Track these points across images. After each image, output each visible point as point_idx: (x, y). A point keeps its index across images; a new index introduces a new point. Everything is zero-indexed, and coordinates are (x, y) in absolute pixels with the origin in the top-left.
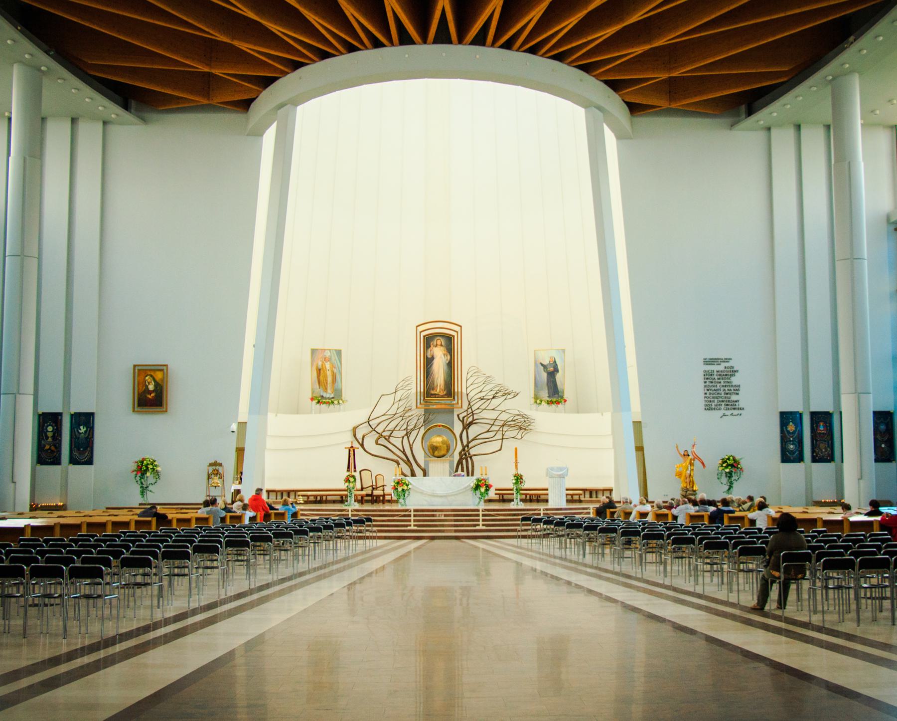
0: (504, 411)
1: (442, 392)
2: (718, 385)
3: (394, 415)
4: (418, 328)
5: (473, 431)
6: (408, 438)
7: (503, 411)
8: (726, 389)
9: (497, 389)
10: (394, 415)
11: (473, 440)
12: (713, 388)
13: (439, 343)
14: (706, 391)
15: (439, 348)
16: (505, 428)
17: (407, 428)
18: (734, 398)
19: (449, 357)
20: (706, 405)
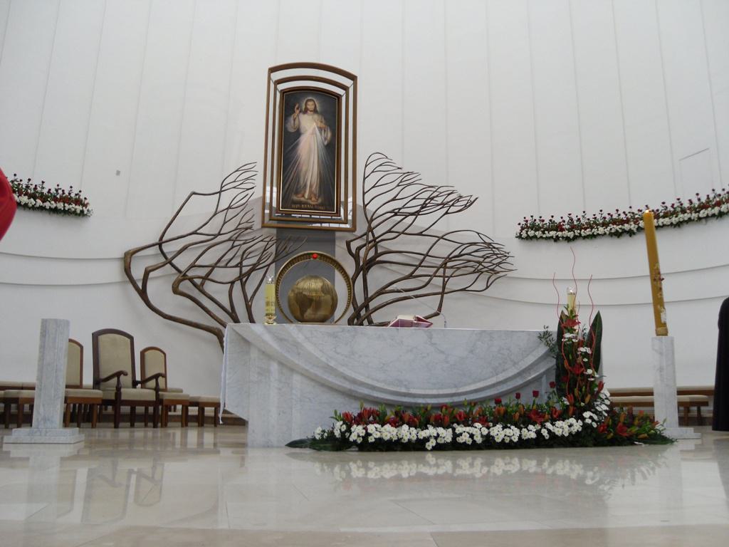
0: (442, 238)
1: (313, 199)
3: (216, 236)
4: (272, 74)
5: (377, 277)
6: (243, 285)
7: (440, 238)
9: (426, 195)
10: (216, 236)
11: (381, 292)
13: (311, 106)
15: (311, 117)
16: (449, 272)
17: (241, 263)
19: (329, 135)
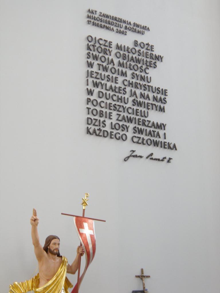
2: (121, 79)
8: (138, 92)
12: (109, 84)
14: (91, 87)
18: (154, 117)
20: (89, 121)
